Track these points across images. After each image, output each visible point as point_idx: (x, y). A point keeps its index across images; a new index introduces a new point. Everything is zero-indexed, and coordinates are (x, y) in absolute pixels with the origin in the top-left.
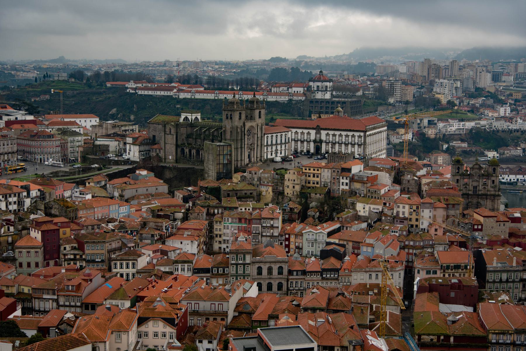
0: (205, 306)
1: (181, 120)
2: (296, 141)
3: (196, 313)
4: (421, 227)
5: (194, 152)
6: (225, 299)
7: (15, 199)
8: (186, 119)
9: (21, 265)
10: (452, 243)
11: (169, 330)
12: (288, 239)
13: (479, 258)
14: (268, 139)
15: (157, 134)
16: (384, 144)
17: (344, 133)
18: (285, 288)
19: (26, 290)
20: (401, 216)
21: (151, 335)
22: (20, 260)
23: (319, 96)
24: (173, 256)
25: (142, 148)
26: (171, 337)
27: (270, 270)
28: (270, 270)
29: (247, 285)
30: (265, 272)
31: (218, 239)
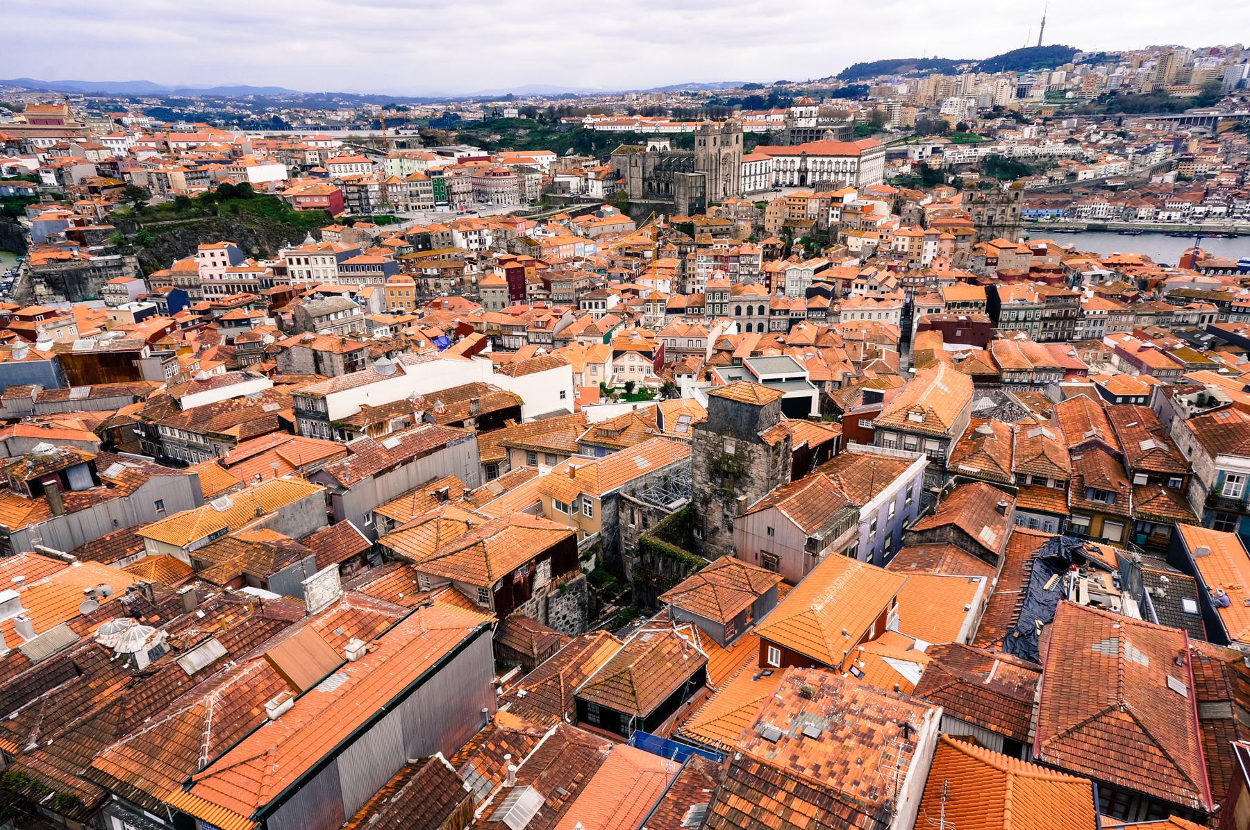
0: (682, 343)
1: (648, 150)
2: (777, 171)
3: (673, 350)
4: (923, 262)
5: (663, 186)
6: (703, 336)
7: (476, 237)
8: (654, 148)
9: (486, 304)
10: (959, 279)
11: (648, 364)
12: (769, 278)
13: (992, 294)
14: (746, 169)
15: (621, 167)
16: (880, 173)
17: (834, 160)
18: (765, 329)
19: (495, 328)
20: (900, 249)
21: (627, 369)
22: (486, 300)
23: (802, 124)
24: (643, 295)
25: (607, 183)
26: (649, 372)
27: (750, 310)
28: (750, 310)
29: (726, 323)
30: (744, 311)
31: (691, 279)
